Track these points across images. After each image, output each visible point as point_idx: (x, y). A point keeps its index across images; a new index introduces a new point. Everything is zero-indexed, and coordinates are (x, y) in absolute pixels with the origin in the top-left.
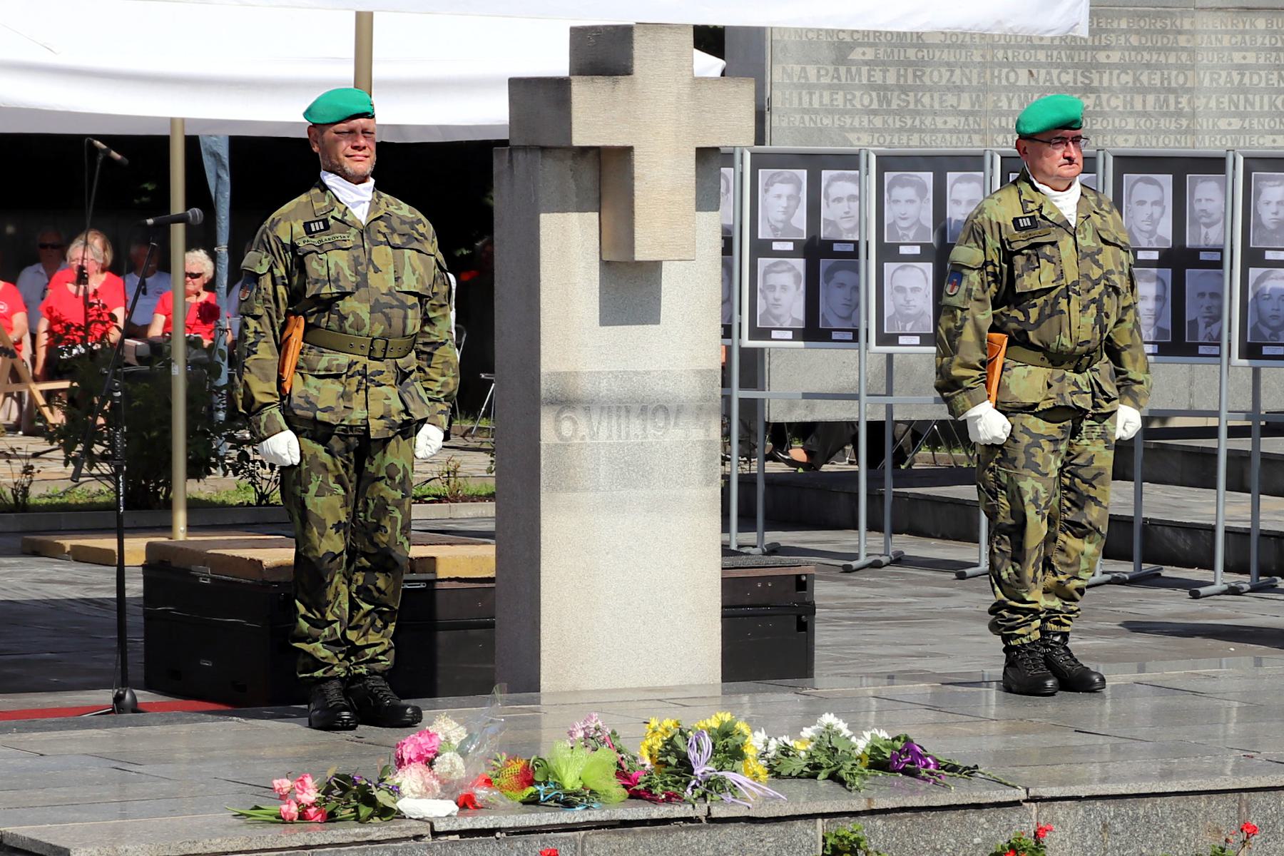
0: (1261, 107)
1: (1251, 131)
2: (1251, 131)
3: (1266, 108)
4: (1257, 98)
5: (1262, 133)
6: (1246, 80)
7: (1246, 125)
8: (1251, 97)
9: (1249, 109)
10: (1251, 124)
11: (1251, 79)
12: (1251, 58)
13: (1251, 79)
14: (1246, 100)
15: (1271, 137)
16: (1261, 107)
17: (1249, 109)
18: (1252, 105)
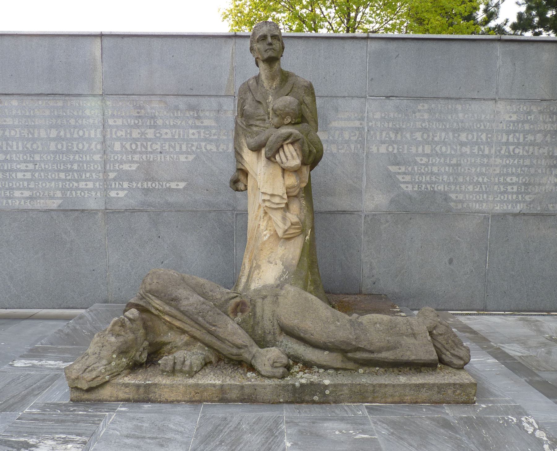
0: (17, 148)
1: (11, 161)
2: (11, 161)
3: (21, 149)
4: (15, 143)
5: (19, 163)
6: (7, 133)
7: (8, 157)
8: (10, 143)
9: (9, 149)
10: (11, 157)
11: (10, 133)
12: (9, 121)
13: (10, 133)
14: (8, 144)
15: (25, 165)
16: (17, 148)
17: (9, 149)
18: (12, 147)
